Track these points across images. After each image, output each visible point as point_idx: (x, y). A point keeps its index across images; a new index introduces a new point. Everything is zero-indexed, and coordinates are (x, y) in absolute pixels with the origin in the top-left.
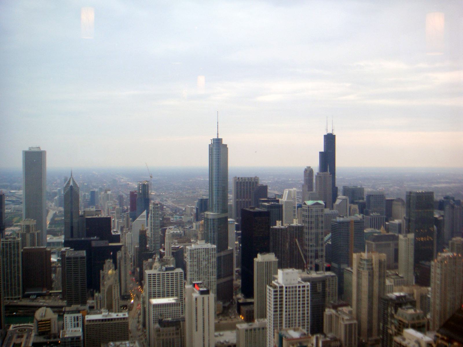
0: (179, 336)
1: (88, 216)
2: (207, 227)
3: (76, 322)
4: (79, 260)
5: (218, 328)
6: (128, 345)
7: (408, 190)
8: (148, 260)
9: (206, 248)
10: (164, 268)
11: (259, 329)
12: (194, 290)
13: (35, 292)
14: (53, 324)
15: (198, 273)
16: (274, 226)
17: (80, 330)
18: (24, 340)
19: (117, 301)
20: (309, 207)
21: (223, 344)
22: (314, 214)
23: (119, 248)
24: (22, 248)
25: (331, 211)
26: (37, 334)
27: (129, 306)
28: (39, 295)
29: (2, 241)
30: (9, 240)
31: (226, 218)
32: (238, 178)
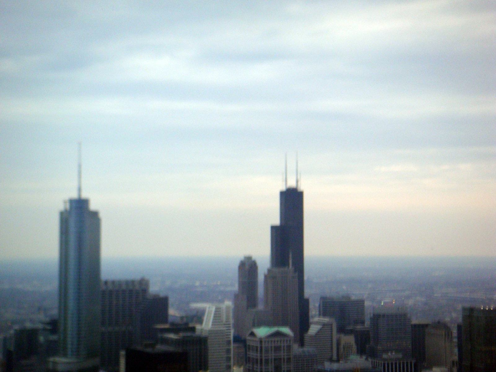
7: (468, 305)
20: (261, 342)
22: (272, 355)
25: (301, 350)
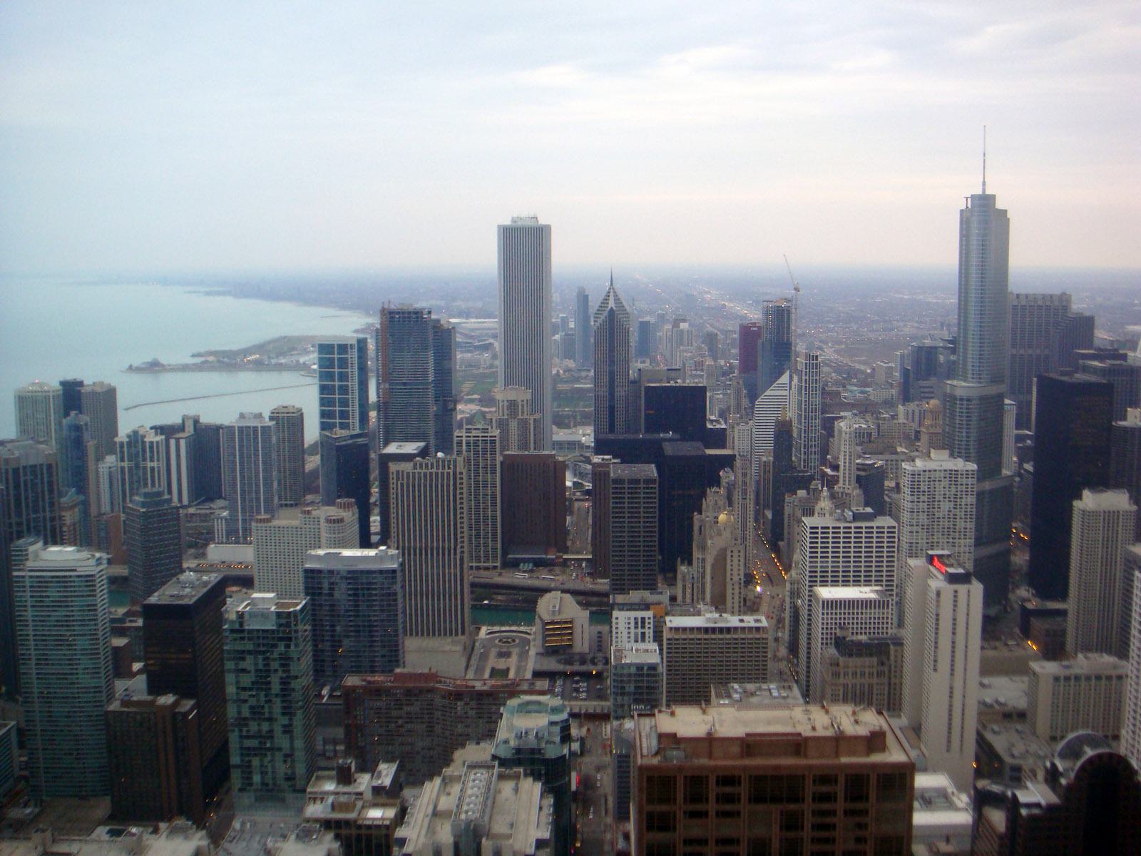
0: (886, 680)
1: (649, 381)
2: (953, 417)
3: (640, 630)
4: (642, 485)
5: (988, 668)
6: (775, 693)
8: (796, 494)
9: (951, 470)
10: (849, 514)
11: (1088, 678)
12: (929, 570)
13: (530, 556)
14: (578, 630)
15: (929, 529)
16: (1121, 420)
17: (655, 650)
18: (512, 662)
19: (736, 587)
21: (991, 706)
23: (729, 461)
24: (501, 454)
26: (541, 650)
27: (750, 600)
28: (539, 563)
29: (458, 437)
30: (474, 433)
31: (1000, 397)
32: (1018, 296)
